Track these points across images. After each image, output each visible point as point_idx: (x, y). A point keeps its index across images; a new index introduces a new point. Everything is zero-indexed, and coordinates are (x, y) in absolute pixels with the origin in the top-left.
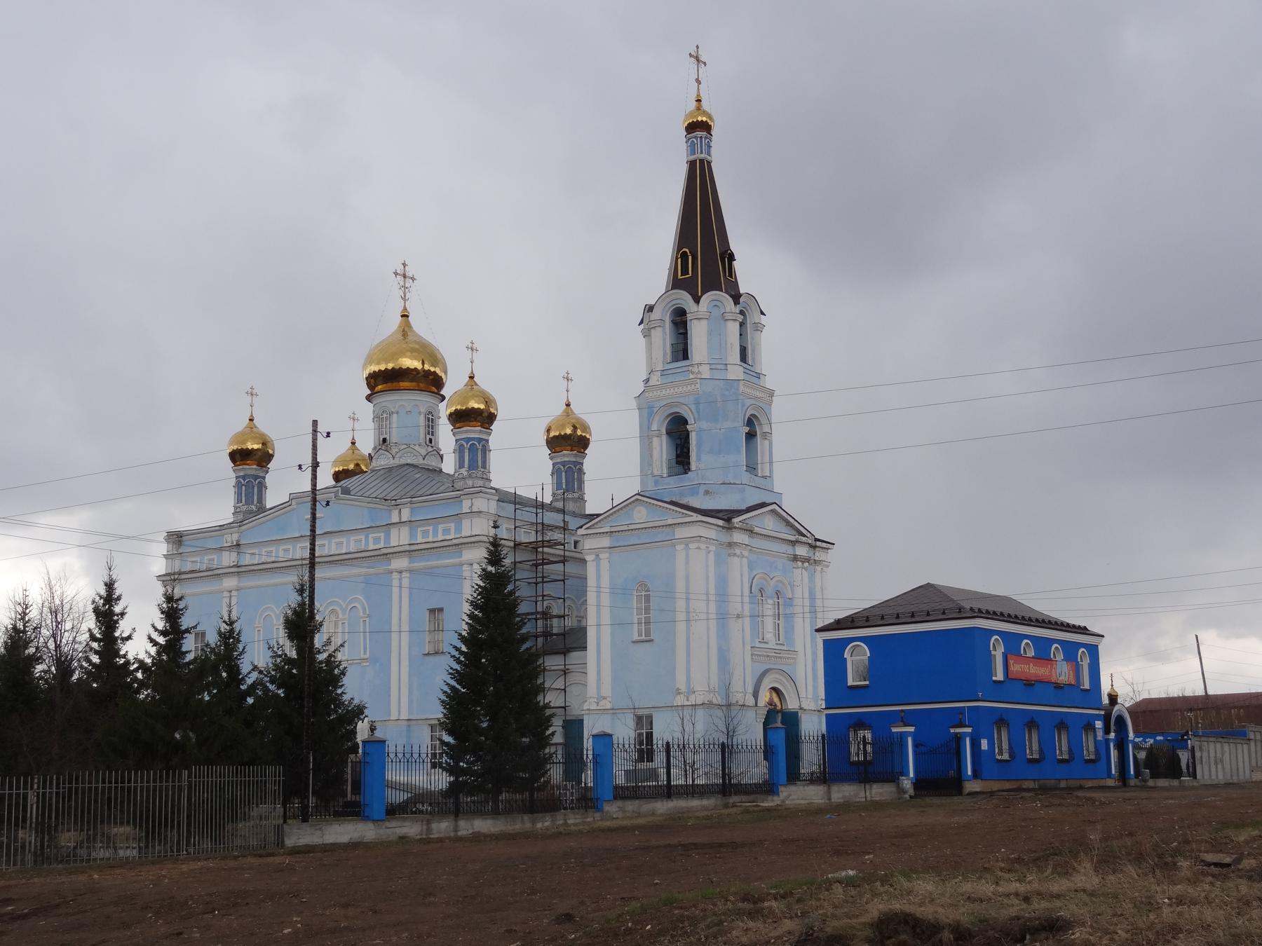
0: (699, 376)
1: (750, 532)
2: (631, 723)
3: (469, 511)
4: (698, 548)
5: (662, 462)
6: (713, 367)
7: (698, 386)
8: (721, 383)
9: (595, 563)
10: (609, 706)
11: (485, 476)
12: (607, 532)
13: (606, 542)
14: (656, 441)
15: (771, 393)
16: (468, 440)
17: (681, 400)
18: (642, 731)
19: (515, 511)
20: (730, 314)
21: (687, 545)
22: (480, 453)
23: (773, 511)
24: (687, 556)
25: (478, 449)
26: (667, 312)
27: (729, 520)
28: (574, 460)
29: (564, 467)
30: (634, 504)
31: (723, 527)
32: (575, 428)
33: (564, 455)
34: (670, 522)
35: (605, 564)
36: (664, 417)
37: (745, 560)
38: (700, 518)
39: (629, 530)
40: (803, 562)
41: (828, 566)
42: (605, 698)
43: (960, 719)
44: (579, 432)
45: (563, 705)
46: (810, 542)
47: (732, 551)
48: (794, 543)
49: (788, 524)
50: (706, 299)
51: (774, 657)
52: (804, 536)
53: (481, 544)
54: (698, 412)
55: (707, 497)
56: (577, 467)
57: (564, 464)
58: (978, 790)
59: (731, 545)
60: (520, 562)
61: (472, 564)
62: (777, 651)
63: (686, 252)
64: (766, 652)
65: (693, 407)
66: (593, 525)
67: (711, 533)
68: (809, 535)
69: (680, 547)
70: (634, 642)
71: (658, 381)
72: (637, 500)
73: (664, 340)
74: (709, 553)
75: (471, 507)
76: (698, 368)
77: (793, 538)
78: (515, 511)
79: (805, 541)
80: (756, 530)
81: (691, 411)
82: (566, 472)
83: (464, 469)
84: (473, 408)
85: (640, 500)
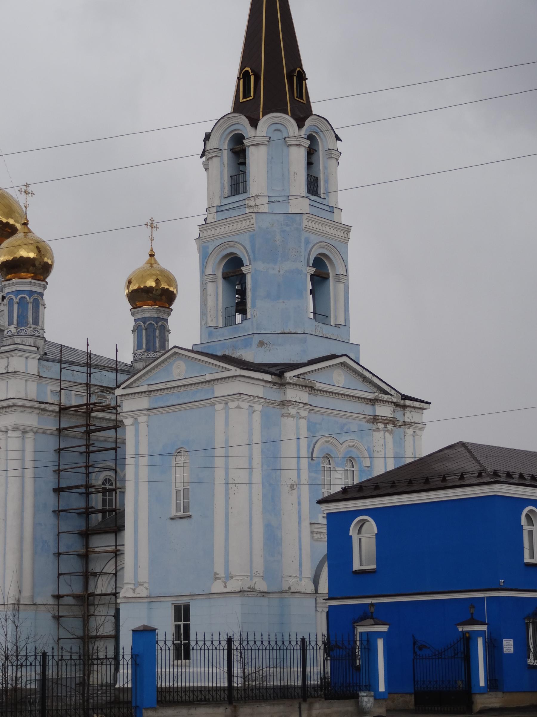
0: (256, 210)
1: (311, 389)
2: (170, 613)
3: (5, 371)
4: (238, 407)
5: (217, 311)
6: (273, 199)
7: (253, 221)
8: (281, 218)
9: (133, 427)
10: (145, 593)
11: (36, 334)
12: (145, 392)
13: (144, 403)
14: (210, 287)
15: (347, 229)
16: (18, 292)
17: (236, 239)
18: (179, 623)
19: (61, 371)
20: (294, 139)
21: (226, 404)
22: (30, 306)
23: (343, 364)
24: (227, 418)
25: (28, 303)
26: (225, 139)
27: (280, 375)
28: (156, 315)
29: (144, 325)
30: (173, 358)
31: (274, 384)
32: (157, 281)
33: (144, 311)
34: (208, 377)
35: (143, 429)
36: (218, 259)
37: (303, 423)
38: (240, 372)
39: (167, 388)
40: (386, 424)
41: (423, 429)
42: (141, 584)
43: (472, 614)
44: (164, 285)
45: (114, 591)
46: (395, 400)
47: (285, 411)
48: (373, 402)
49: (365, 379)
50: (265, 122)
52: (387, 393)
53: (15, 408)
54: (254, 252)
55: (262, 349)
56: (160, 324)
57: (144, 320)
58: (497, 705)
59: (283, 404)
60: (66, 429)
61: (7, 432)
63: (247, 71)
65: (248, 247)
66: (131, 383)
67: (258, 390)
68: (393, 392)
69: (219, 407)
70: (172, 519)
71: (214, 218)
72: (176, 353)
73: (222, 172)
74: (253, 413)
75: (7, 367)
76: (255, 201)
77: (371, 396)
78: (61, 371)
79: (388, 400)
80: (318, 386)
81: (245, 248)
82: (146, 329)
83: (13, 326)
84: (22, 257)
85: (180, 354)
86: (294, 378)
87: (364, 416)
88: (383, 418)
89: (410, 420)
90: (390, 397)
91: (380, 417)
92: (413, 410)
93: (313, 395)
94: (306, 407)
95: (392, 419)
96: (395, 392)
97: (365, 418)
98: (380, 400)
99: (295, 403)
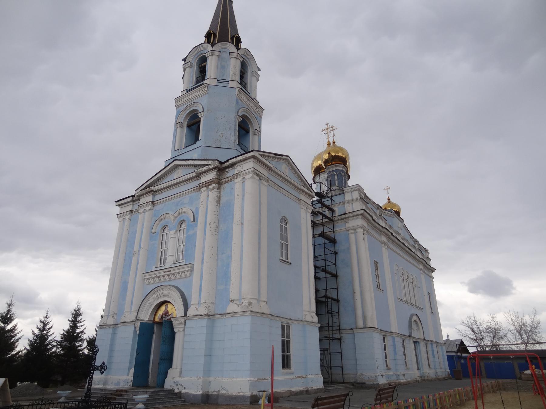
40: (207, 186)
46: (211, 167)
48: (199, 176)
51: (164, 276)
62: (164, 271)
77: (194, 174)
79: (206, 169)
86: (139, 192)
90: (207, 167)
91: (201, 184)
92: (243, 163)
93: (159, 194)
94: (148, 204)
95: (211, 180)
96: (212, 161)
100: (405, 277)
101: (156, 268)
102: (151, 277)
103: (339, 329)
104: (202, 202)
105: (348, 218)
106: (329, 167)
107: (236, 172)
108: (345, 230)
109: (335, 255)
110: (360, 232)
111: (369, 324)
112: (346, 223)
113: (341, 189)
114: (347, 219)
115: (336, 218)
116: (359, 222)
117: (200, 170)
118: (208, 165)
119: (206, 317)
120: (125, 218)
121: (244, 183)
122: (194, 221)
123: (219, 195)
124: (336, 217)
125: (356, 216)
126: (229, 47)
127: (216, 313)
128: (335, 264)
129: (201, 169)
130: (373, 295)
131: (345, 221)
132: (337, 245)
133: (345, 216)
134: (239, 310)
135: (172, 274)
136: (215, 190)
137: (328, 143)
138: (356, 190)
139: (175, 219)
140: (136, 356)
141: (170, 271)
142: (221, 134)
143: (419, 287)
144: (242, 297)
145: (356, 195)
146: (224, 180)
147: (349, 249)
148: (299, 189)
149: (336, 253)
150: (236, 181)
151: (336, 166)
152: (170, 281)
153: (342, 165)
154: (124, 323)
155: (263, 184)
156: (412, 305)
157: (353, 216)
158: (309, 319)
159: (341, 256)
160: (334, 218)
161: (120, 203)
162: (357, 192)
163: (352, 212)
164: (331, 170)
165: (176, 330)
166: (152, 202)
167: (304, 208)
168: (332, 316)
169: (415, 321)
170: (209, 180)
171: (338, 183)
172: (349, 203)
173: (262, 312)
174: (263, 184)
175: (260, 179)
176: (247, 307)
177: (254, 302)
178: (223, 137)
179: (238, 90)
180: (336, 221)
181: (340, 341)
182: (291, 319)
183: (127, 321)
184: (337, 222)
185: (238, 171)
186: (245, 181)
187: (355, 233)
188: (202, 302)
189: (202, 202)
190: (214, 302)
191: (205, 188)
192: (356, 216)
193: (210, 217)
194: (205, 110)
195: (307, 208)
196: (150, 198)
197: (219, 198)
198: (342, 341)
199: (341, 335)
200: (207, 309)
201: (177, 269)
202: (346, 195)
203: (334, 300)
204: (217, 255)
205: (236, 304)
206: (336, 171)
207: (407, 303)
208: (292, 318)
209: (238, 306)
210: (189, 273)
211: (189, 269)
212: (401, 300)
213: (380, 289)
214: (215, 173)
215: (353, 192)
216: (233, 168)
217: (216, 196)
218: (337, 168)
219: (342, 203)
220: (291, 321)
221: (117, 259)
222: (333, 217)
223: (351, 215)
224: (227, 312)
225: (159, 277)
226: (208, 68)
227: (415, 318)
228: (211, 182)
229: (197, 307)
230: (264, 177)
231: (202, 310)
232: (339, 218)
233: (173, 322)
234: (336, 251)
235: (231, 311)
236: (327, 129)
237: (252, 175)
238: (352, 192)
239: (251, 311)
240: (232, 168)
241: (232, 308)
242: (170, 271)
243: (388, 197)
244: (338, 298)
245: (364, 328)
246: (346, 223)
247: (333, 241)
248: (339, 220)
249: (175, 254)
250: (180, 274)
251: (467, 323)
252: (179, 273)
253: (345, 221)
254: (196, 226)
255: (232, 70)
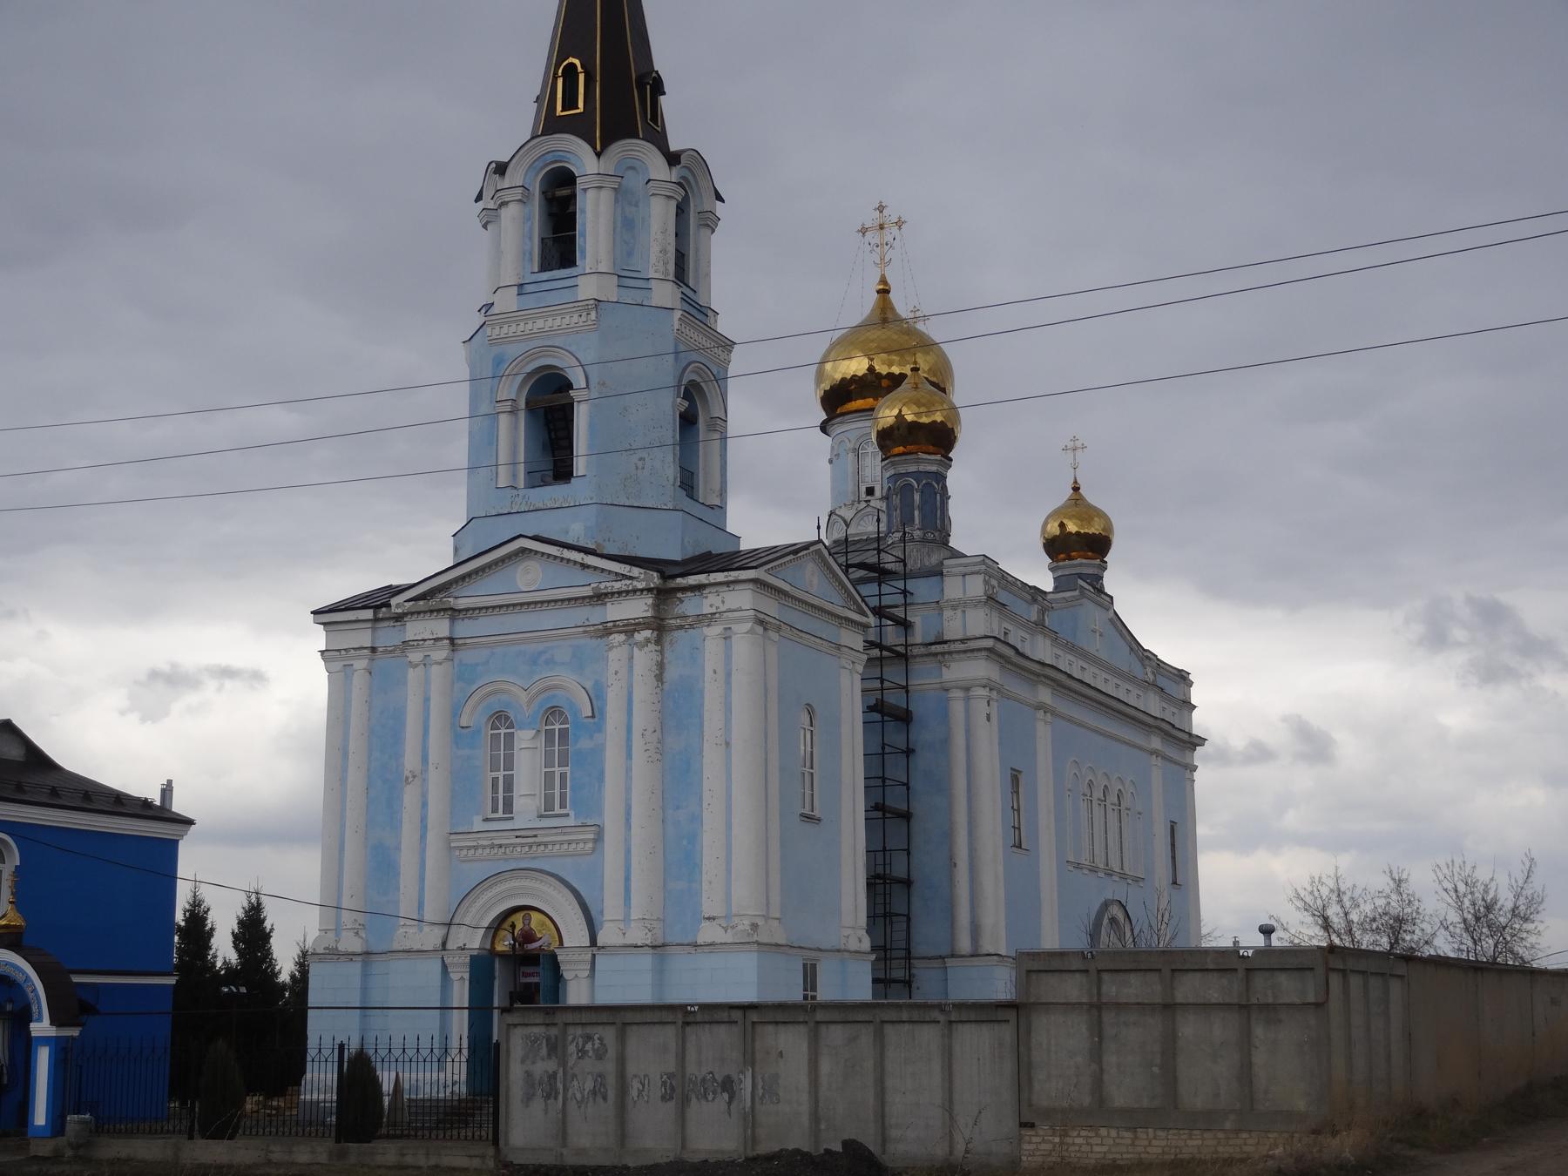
46: (640, 585)
48: (600, 598)
51: (514, 846)
62: (518, 833)
64: (484, 839)
77: (587, 591)
79: (624, 588)
86: (406, 604)
87: (581, 629)
88: (617, 623)
89: (717, 608)
90: (628, 582)
91: (609, 625)
92: (725, 588)
93: (470, 618)
94: (439, 644)
95: (641, 620)
96: (642, 571)
97: (585, 632)
98: (613, 594)
99: (415, 643)
100: (1098, 794)
101: (484, 820)
102: (475, 844)
103: (909, 957)
104: (616, 673)
105: (950, 653)
106: (897, 459)
107: (707, 610)
108: (938, 686)
109: (908, 757)
110: (981, 697)
111: (987, 946)
112: (944, 669)
113: (930, 536)
114: (946, 656)
115: (916, 651)
116: (978, 669)
117: (606, 587)
118: (631, 578)
119: (651, 951)
120: (352, 665)
121: (728, 641)
122: (593, 716)
123: (659, 659)
124: (917, 647)
125: (972, 651)
126: (644, 154)
127: (669, 940)
128: (907, 785)
129: (608, 584)
130: (1001, 868)
131: (940, 662)
132: (914, 728)
133: (941, 648)
134: (728, 938)
135: (539, 844)
136: (652, 647)
137: (881, 287)
138: (978, 573)
139: (530, 702)
140: (469, 1030)
141: (535, 836)
142: (640, 459)
143: (1139, 813)
144: (734, 910)
145: (976, 587)
146: (671, 622)
147: (946, 742)
148: (841, 618)
149: (909, 752)
150: (706, 631)
151: (918, 461)
152: (534, 858)
153: (938, 457)
154: (404, 951)
155: (770, 639)
156: (1109, 873)
157: (965, 652)
158: (853, 945)
159: (921, 761)
160: (909, 648)
161: (328, 615)
162: (981, 577)
163: (962, 641)
164: (902, 469)
165: (566, 975)
166: (452, 640)
167: (848, 667)
168: (891, 923)
169: (1113, 920)
170: (634, 619)
171: (923, 517)
172: (954, 608)
173: (773, 941)
174: (770, 639)
175: (765, 629)
176: (749, 934)
177: (760, 922)
178: (643, 468)
179: (679, 316)
180: (915, 657)
181: (910, 987)
182: (820, 950)
183: (415, 948)
184: (918, 660)
185: (711, 606)
186: (730, 637)
187: (967, 699)
188: (633, 916)
189: (616, 673)
190: (661, 917)
191: (622, 637)
192: (972, 651)
193: (643, 718)
194: (594, 380)
195: (853, 662)
196: (441, 627)
197: (661, 666)
198: (914, 985)
199: (913, 971)
200: (650, 934)
201: (556, 834)
202: (948, 581)
203: (899, 881)
204: (663, 809)
205: (720, 925)
206: (917, 475)
207: (1094, 870)
208: (822, 947)
209: (726, 931)
210: (590, 845)
211: (592, 836)
212: (1078, 866)
213: (1020, 847)
214: (650, 601)
215: (967, 577)
216: (697, 594)
217: (654, 662)
218: (922, 468)
219: (934, 605)
220: (819, 954)
221: (343, 780)
222: (906, 646)
223: (961, 647)
224: (700, 941)
225: (500, 846)
226: (584, 224)
227: (1116, 911)
228: (639, 624)
229: (622, 927)
230: (775, 621)
231: (638, 935)
232: (923, 650)
233: (559, 958)
234: (910, 746)
235: (709, 941)
236: (881, 227)
237: (752, 626)
238: (964, 576)
239: (759, 944)
240: (692, 592)
241: (708, 933)
242: (535, 836)
243: (1076, 482)
244: (909, 876)
245: (972, 956)
246: (944, 669)
247: (904, 718)
248: (922, 656)
249: (538, 793)
250: (565, 846)
251: (1309, 899)
252: (561, 843)
253: (940, 662)
254: (600, 728)
255: (655, 240)
